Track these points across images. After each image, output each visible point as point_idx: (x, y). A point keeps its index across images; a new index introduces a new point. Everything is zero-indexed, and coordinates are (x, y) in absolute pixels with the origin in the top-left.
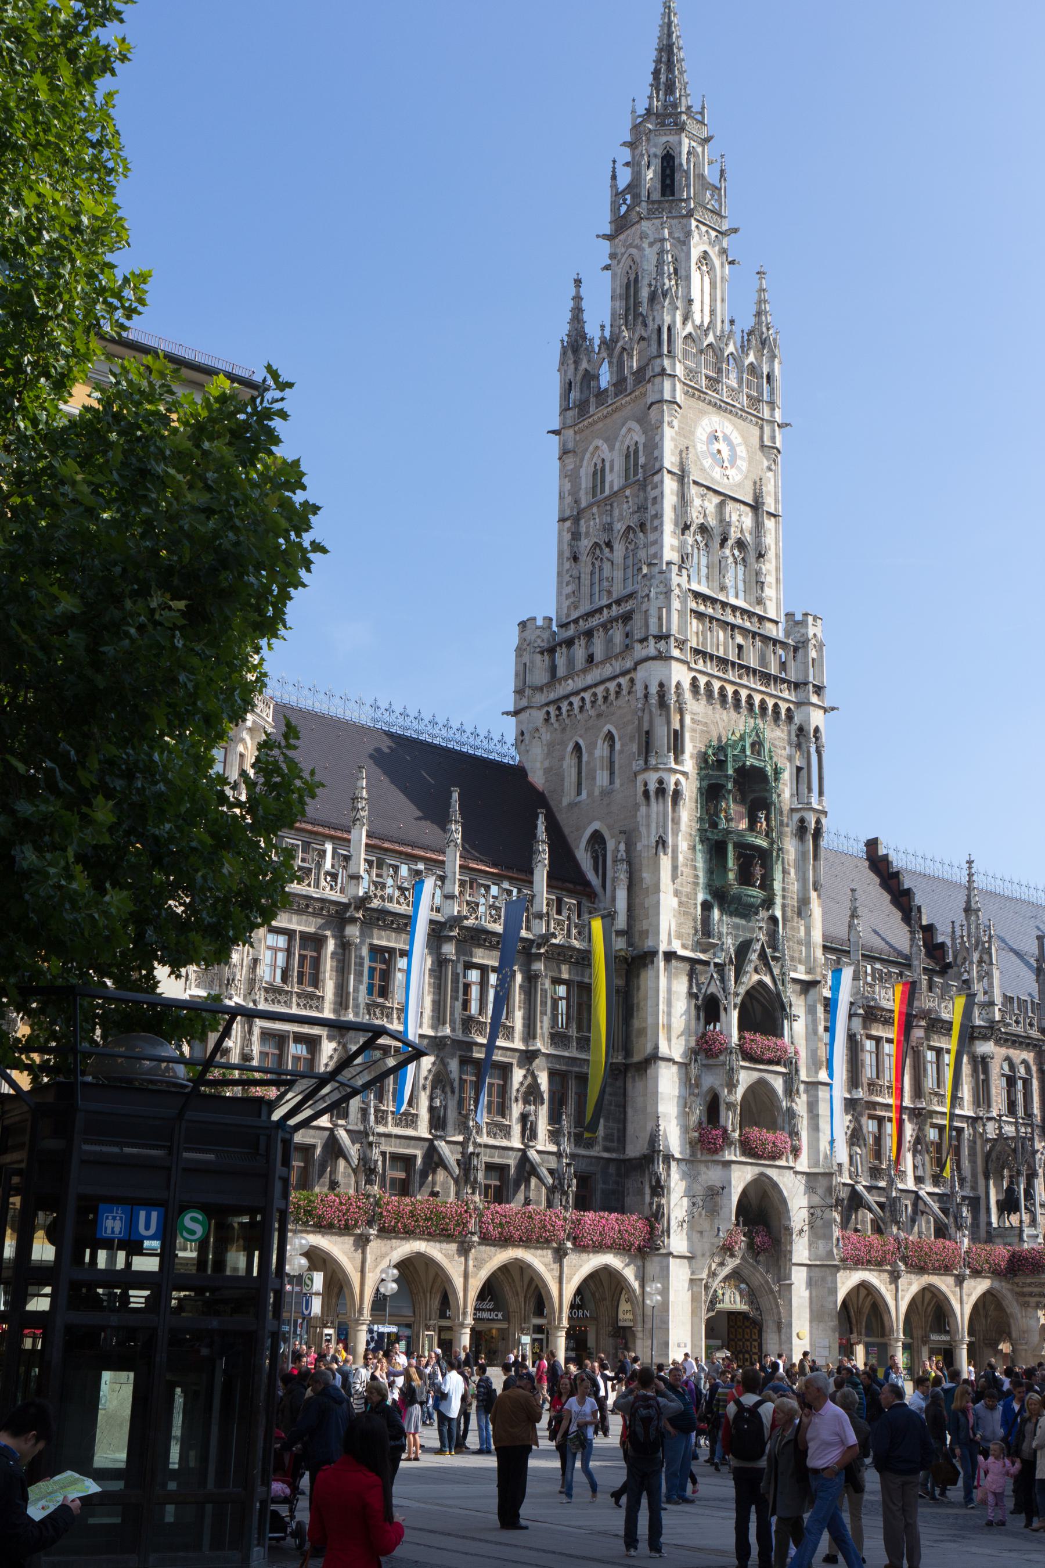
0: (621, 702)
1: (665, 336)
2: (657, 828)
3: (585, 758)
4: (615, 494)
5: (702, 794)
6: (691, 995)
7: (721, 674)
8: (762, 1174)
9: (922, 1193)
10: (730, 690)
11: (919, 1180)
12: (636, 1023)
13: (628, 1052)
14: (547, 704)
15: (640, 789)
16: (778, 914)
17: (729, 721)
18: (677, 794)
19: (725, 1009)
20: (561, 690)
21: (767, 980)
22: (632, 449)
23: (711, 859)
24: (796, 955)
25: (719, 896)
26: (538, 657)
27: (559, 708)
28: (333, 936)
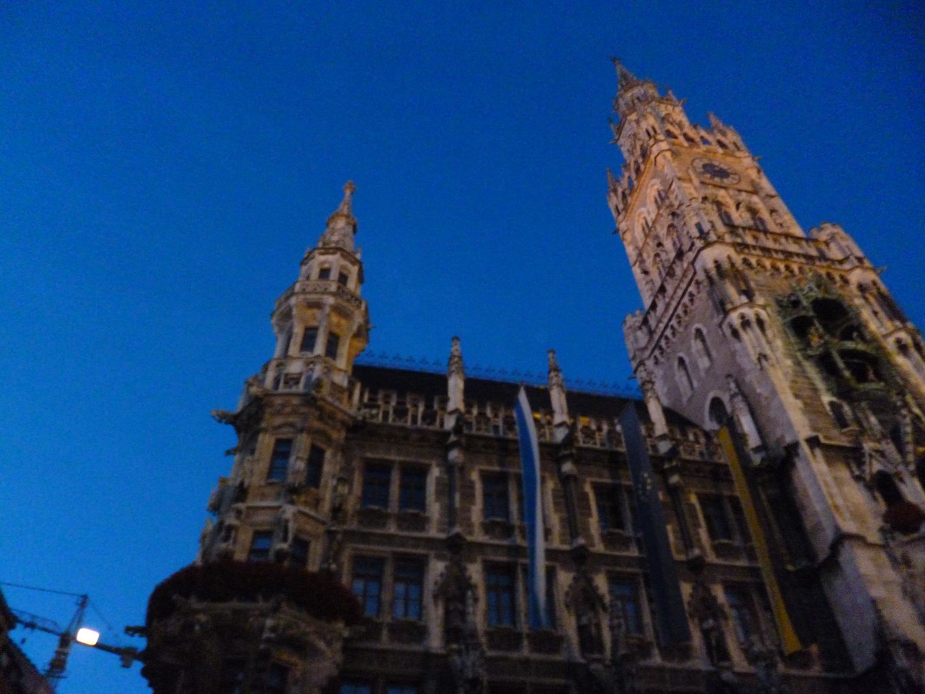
0: (697, 303)
2: (754, 347)
3: (687, 360)
4: (654, 222)
5: (789, 327)
6: (858, 479)
10: (782, 266)
12: (808, 524)
13: (810, 554)
14: (652, 352)
15: (728, 332)
16: (917, 410)
18: (760, 322)
19: (902, 480)
20: (656, 337)
22: (657, 196)
25: (844, 392)
26: (639, 333)
27: (661, 348)
28: (438, 465)
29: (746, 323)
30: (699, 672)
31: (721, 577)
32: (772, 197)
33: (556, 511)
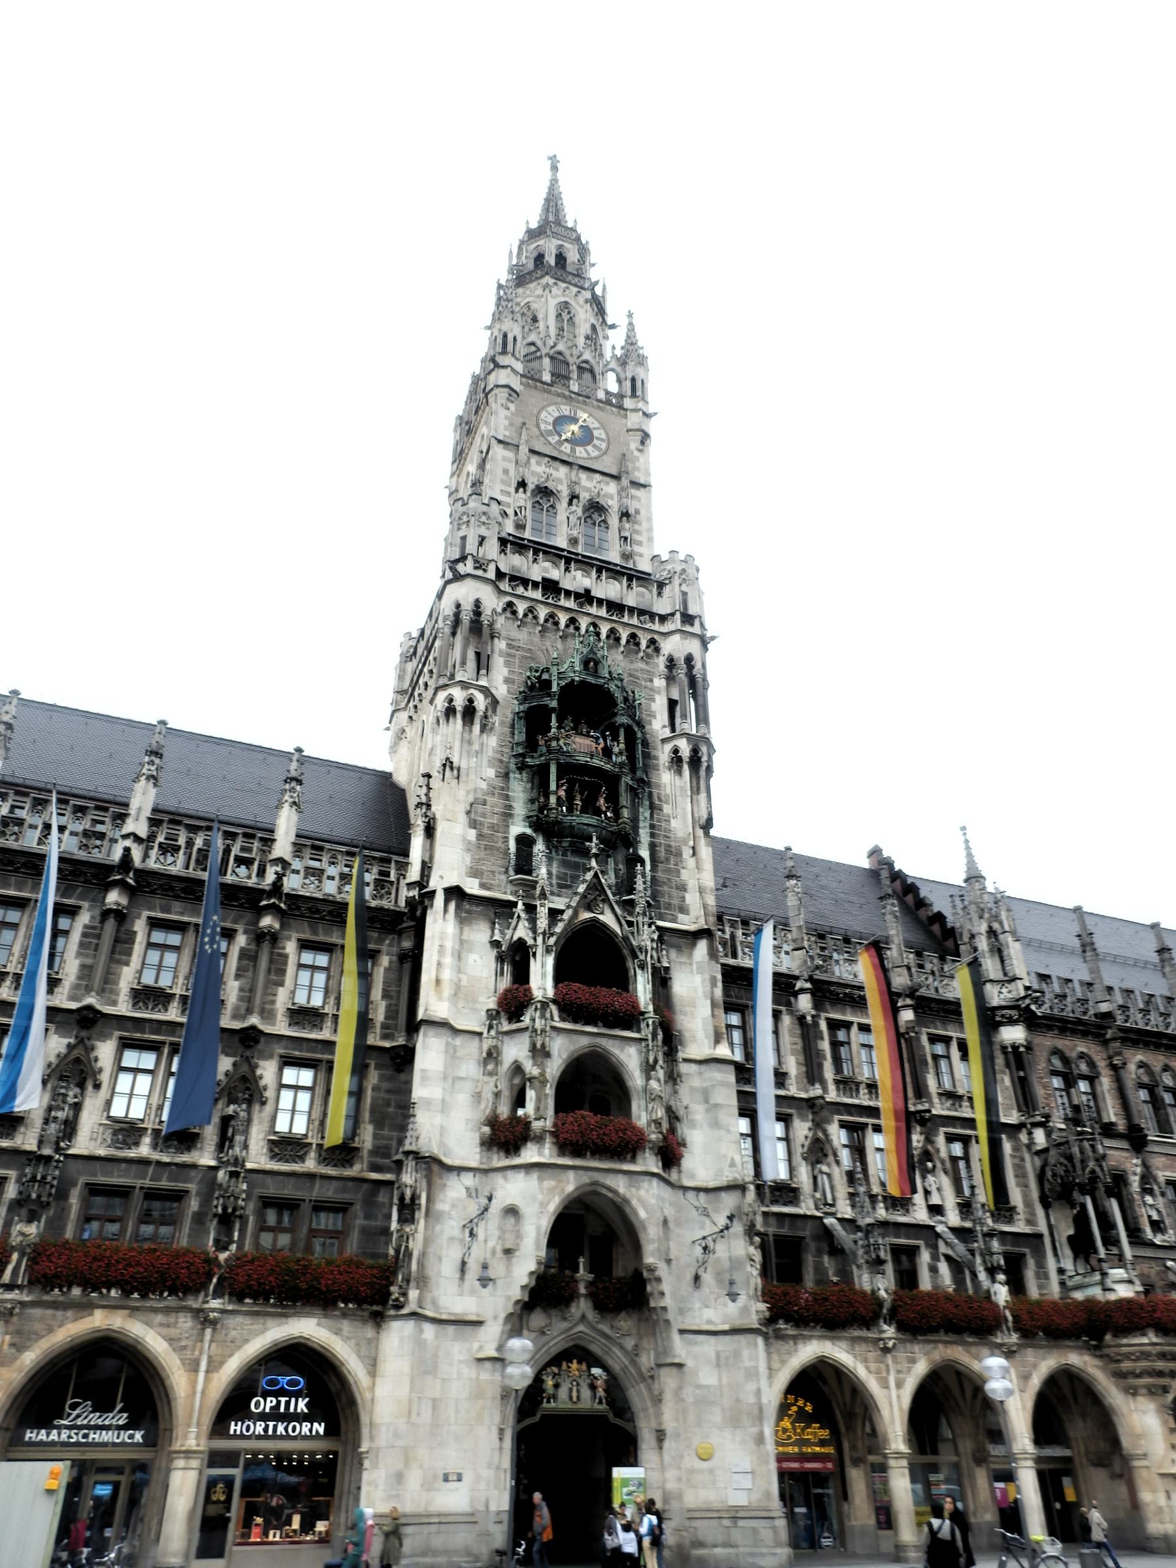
1: (500, 340)
5: (520, 718)
6: (495, 944)
7: (550, 601)
8: (596, 1183)
9: (940, 1229)
11: (936, 1210)
14: (409, 701)
16: (644, 853)
17: (565, 650)
18: (469, 711)
19: (534, 954)
21: (608, 918)
23: (532, 788)
24: (675, 902)
25: (542, 824)
29: (450, 711)
30: (194, 1166)
31: (282, 1051)
32: (644, 486)
33: (79, 954)
